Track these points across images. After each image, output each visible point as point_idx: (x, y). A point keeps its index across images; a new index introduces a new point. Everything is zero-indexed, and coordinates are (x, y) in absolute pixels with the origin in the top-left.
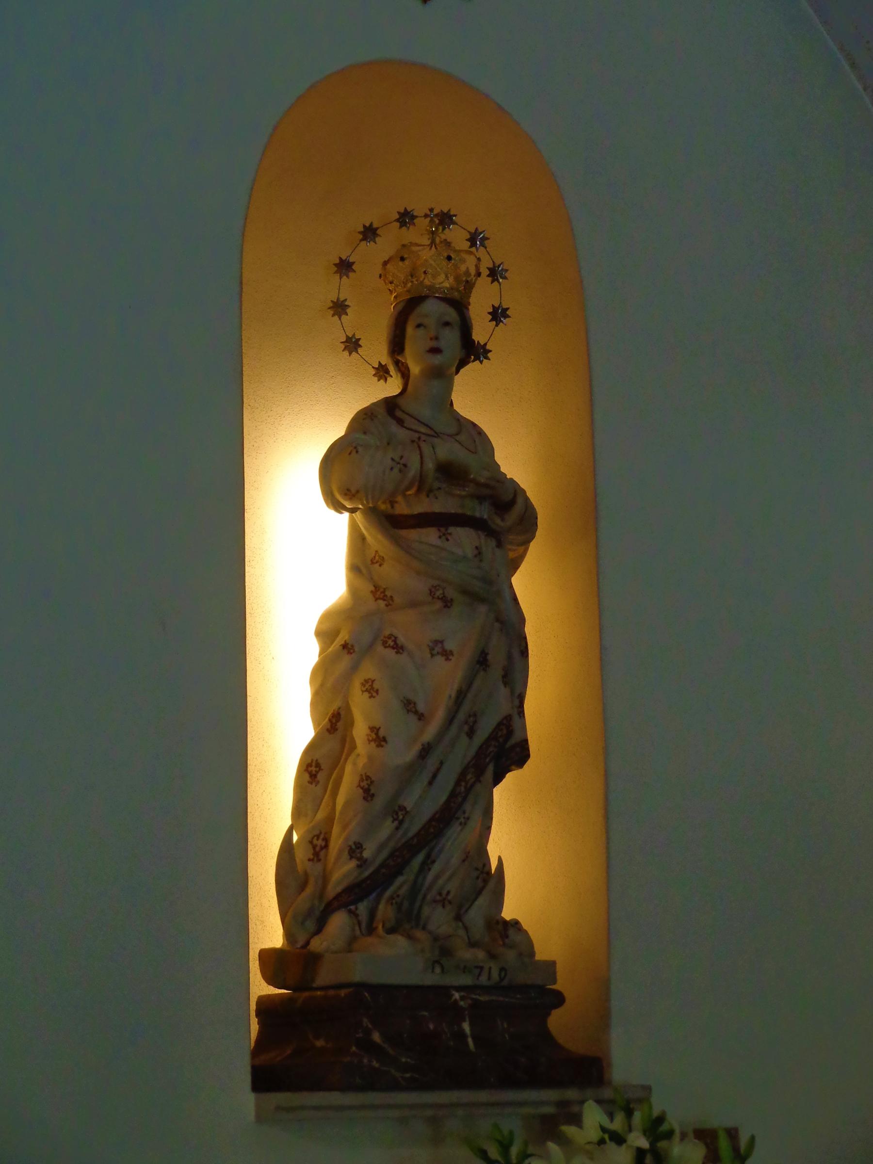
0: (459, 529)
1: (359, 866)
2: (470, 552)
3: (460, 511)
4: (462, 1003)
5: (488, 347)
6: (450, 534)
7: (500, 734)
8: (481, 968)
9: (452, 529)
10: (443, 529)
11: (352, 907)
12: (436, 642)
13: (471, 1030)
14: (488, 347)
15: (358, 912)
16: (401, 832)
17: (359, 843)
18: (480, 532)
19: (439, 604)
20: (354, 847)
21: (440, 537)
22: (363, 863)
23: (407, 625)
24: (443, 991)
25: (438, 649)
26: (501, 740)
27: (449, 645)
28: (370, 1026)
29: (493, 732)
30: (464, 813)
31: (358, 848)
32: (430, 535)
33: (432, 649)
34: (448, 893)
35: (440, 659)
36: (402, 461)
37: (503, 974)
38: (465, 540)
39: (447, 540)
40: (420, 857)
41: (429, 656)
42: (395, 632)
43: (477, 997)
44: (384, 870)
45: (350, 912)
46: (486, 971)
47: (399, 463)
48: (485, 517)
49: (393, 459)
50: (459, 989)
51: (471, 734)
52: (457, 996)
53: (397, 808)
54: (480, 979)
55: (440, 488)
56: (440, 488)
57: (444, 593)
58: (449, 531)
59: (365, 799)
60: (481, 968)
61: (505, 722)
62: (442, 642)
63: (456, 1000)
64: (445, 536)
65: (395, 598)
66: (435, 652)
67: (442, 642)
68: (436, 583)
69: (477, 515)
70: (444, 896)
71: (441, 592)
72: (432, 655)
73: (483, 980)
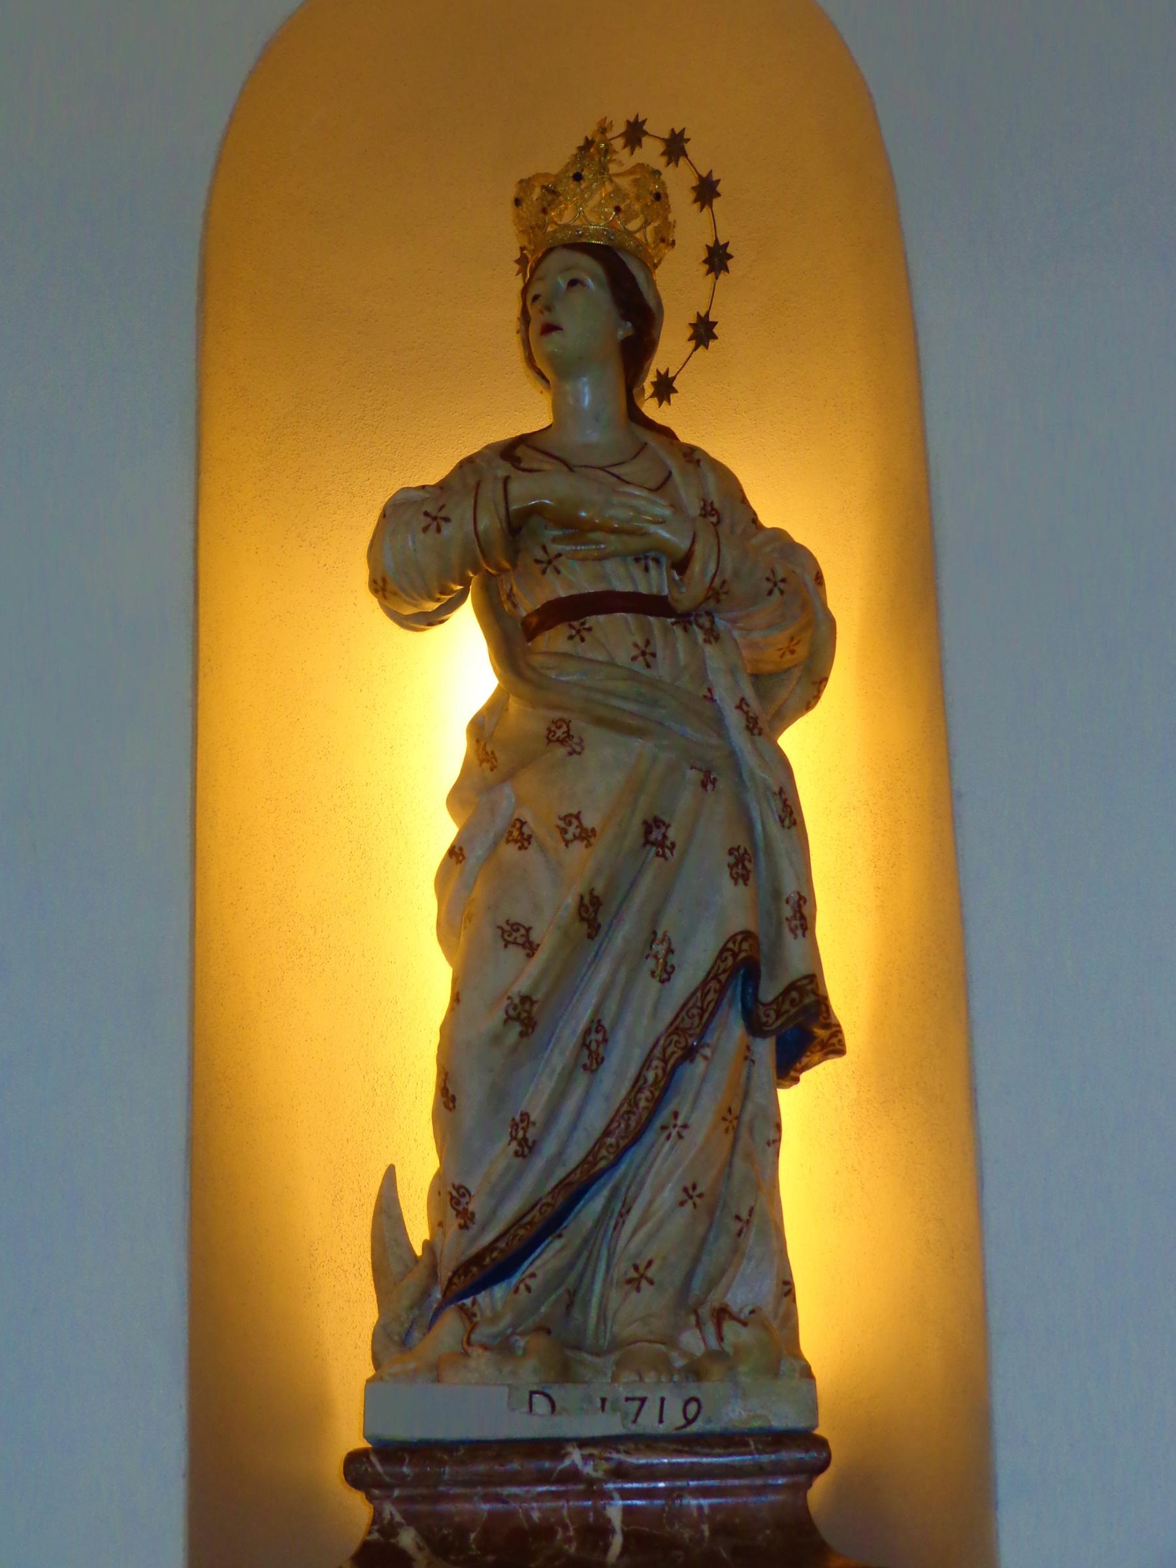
0: (602, 618)
1: (464, 1227)
2: (623, 656)
3: (600, 587)
4: (588, 1469)
5: (711, 319)
6: (590, 629)
7: (722, 966)
8: (643, 1400)
9: (591, 620)
10: (576, 624)
11: (468, 1302)
12: (568, 819)
13: (624, 1522)
14: (711, 319)
15: (476, 1309)
16: (539, 1163)
17: (461, 1187)
18: (630, 617)
19: (561, 751)
20: (455, 1193)
21: (571, 638)
22: (466, 1219)
23: (536, 799)
24: (554, 1447)
25: (572, 830)
26: (723, 978)
27: (589, 821)
28: (398, 1518)
29: (712, 967)
30: (676, 1115)
31: (463, 1195)
32: (556, 639)
33: (564, 831)
34: (650, 1263)
35: (578, 847)
36: (443, 514)
37: (692, 1408)
38: (616, 634)
39: (583, 640)
40: (593, 1207)
41: (563, 845)
42: (526, 815)
43: (623, 1457)
44: (522, 1232)
45: (462, 1308)
46: (651, 1409)
47: (435, 518)
48: (666, 592)
49: (426, 514)
50: (582, 1443)
51: (666, 974)
52: (575, 1456)
53: (518, 1118)
54: (639, 1420)
55: (559, 555)
56: (559, 555)
57: (568, 732)
58: (587, 626)
59: (447, 1107)
60: (643, 1400)
61: (730, 945)
62: (577, 816)
63: (574, 1465)
64: (579, 635)
65: (497, 754)
66: (569, 836)
67: (577, 816)
68: (557, 715)
69: (643, 589)
70: (641, 1269)
71: (564, 728)
72: (567, 843)
73: (648, 1422)
